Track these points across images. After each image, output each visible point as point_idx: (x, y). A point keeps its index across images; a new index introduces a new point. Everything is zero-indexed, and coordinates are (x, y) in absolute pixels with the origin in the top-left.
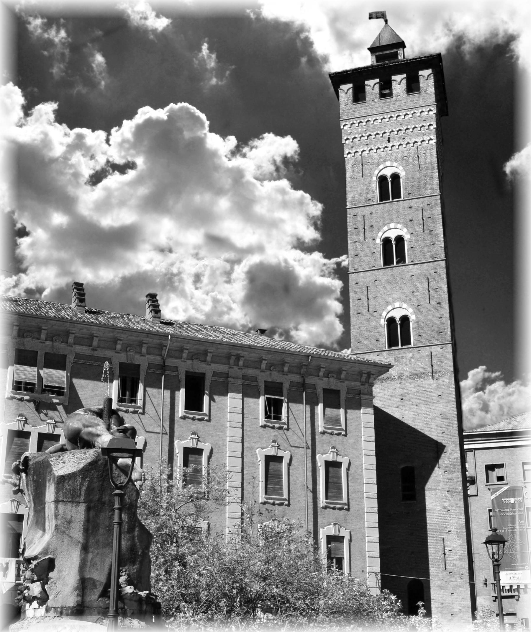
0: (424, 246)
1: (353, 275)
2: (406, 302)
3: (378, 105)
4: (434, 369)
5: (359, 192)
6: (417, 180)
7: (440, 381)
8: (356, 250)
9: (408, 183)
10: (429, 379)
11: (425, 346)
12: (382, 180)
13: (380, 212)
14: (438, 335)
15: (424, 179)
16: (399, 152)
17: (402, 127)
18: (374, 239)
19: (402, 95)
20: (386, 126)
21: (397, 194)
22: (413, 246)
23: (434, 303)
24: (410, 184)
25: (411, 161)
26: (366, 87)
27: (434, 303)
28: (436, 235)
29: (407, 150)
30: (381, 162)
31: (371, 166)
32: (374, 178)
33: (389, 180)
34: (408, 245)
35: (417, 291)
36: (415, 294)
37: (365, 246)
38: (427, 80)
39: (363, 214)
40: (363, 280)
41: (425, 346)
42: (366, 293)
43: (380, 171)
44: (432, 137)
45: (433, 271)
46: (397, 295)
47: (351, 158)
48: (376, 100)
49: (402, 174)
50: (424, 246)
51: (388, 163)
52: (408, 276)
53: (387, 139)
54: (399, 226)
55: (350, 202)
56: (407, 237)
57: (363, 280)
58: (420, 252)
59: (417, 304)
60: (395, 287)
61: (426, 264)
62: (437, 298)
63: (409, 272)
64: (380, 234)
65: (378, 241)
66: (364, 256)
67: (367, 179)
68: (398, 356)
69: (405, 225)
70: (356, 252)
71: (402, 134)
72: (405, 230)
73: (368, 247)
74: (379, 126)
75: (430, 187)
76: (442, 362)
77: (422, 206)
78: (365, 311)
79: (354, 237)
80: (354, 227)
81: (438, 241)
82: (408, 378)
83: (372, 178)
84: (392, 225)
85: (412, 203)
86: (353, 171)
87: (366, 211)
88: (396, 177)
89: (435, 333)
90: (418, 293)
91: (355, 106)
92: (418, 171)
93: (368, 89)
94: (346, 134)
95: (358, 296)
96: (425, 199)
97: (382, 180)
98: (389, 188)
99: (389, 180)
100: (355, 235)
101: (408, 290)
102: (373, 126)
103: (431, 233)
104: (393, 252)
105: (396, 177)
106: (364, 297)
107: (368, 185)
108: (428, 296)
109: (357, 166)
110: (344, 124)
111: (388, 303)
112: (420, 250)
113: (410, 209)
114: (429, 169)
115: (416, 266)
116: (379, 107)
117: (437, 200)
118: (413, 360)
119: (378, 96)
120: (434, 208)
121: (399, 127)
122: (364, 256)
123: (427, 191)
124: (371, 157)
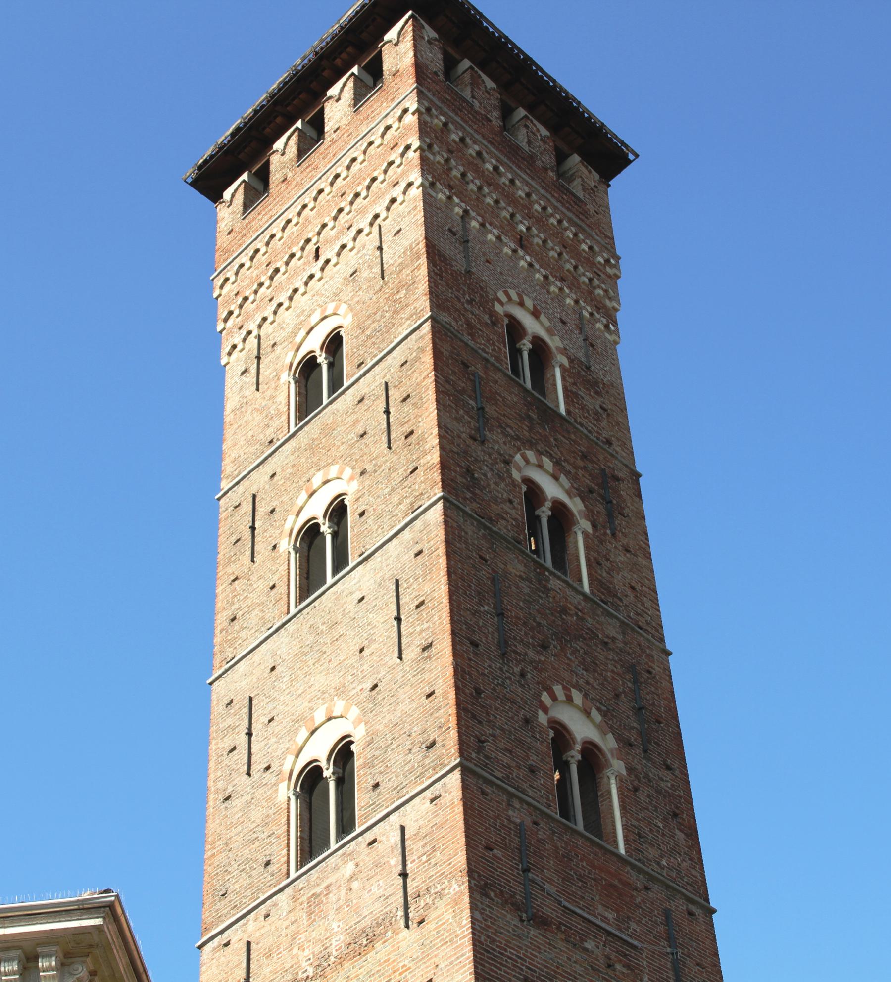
0: (393, 490)
4: (412, 885)
7: (430, 926)
10: (396, 932)
11: (387, 815)
14: (425, 757)
23: (411, 653)
35: (372, 641)
36: (366, 652)
37: (254, 578)
41: (387, 815)
46: (320, 681)
54: (333, 471)
59: (369, 685)
62: (422, 631)
68: (318, 890)
73: (260, 578)
76: (434, 849)
81: (425, 453)
82: (341, 960)
89: (417, 756)
90: (374, 646)
95: (227, 744)
118: (355, 885)
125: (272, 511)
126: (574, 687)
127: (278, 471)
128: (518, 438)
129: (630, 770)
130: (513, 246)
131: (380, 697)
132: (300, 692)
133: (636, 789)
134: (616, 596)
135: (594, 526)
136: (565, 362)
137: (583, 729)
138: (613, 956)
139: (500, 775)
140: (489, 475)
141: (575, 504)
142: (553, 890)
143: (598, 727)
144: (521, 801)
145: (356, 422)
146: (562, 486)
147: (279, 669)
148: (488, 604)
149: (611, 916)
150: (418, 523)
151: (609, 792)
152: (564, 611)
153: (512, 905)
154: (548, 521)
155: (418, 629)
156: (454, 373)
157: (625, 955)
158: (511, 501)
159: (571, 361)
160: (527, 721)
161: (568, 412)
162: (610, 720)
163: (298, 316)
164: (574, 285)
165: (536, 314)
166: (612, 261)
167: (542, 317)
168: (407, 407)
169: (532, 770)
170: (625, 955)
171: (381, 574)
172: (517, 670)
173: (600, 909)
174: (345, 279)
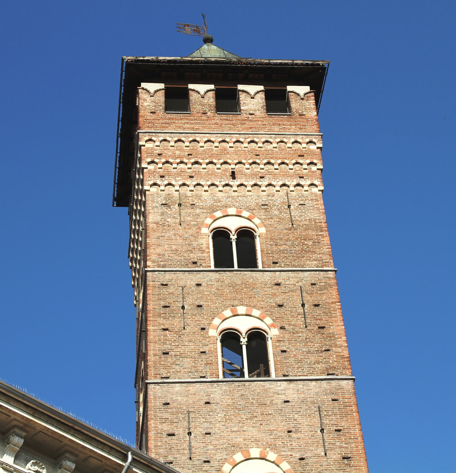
0: (309, 352)
1: (157, 387)
2: (274, 448)
3: (213, 122)
5: (174, 247)
6: (289, 243)
8: (165, 343)
9: (271, 245)
12: (220, 236)
13: (215, 283)
15: (303, 244)
16: (254, 197)
17: (259, 159)
18: (203, 329)
19: (258, 113)
20: (228, 153)
21: (248, 261)
22: (284, 349)
24: (275, 248)
25: (276, 212)
26: (191, 92)
27: (334, 456)
28: (331, 336)
29: (268, 196)
30: (218, 206)
31: (198, 211)
32: (205, 230)
33: (233, 237)
34: (274, 347)
37: (185, 338)
38: (302, 99)
39: (182, 283)
40: (179, 398)
42: (186, 424)
43: (215, 221)
44: (316, 182)
45: (330, 397)
47: (158, 194)
48: (209, 113)
49: (260, 231)
50: (309, 352)
51: (232, 211)
52: (280, 402)
53: (229, 174)
54: (256, 313)
55: (154, 262)
56: (273, 333)
57: (179, 398)
58: (300, 361)
59: (298, 456)
60: (251, 419)
61: (314, 383)
63: (278, 394)
64: (217, 321)
65: (214, 333)
66: (182, 356)
67: (190, 228)
69: (267, 312)
70: (166, 347)
71: (259, 170)
72: (268, 320)
73: (190, 341)
74: (214, 152)
75: (315, 256)
77: (300, 284)
78: (185, 458)
79: (161, 320)
80: (163, 303)
81: (336, 346)
83: (200, 228)
84: (241, 310)
85: (280, 277)
86: (162, 214)
87: (190, 280)
88: (246, 235)
90: (299, 435)
91: (169, 116)
92: (290, 229)
93: (193, 97)
94: (150, 152)
95: (167, 428)
96: (306, 274)
97: (220, 236)
98: (234, 250)
99: (233, 237)
100: (164, 318)
101: (279, 425)
102: (204, 151)
103: (321, 330)
104: (249, 354)
105: (246, 235)
106: (181, 431)
107: (193, 239)
108: (321, 441)
109: (169, 207)
110: (147, 138)
111: (234, 448)
112: (300, 357)
113: (277, 287)
114: (312, 229)
115: (292, 385)
116: (216, 124)
117: (329, 278)
119: (213, 108)
120: (325, 291)
121: (251, 158)
122: (182, 356)
123: (308, 262)
124: (199, 197)
125: (200, 306)
127: (204, 284)
131: (308, 468)
132: (235, 429)
145: (274, 295)
147: (213, 406)
150: (334, 383)
155: (338, 444)
163: (215, 201)
168: (318, 311)
171: (302, 396)
174: (257, 204)
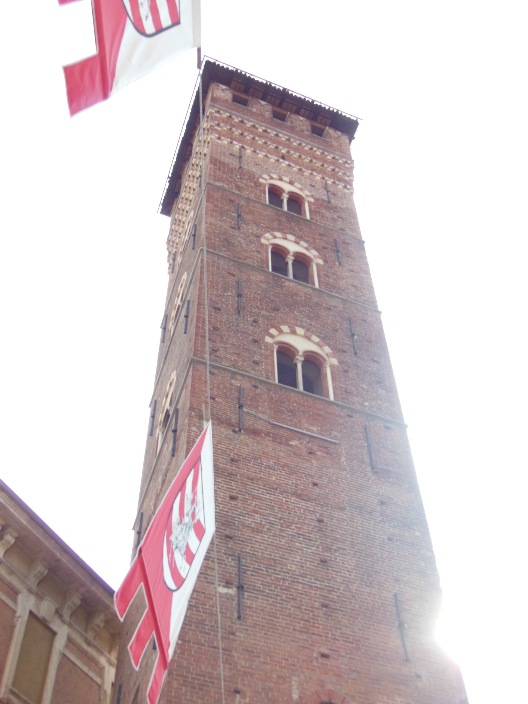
126: (298, 326)
128: (269, 228)
129: (341, 362)
130: (276, 158)
133: (346, 371)
134: (340, 289)
135: (325, 261)
136: (312, 200)
137: (302, 344)
138: (315, 448)
139: (227, 364)
140: (242, 241)
141: (311, 253)
142: (265, 417)
143: (317, 344)
144: (243, 376)
146: (302, 246)
148: (232, 292)
149: (315, 429)
151: (326, 374)
152: (296, 295)
153: (227, 424)
154: (293, 264)
156: (222, 204)
157: (326, 448)
158: (258, 252)
159: (316, 199)
160: (255, 341)
161: (311, 218)
162: (325, 340)
164: (322, 171)
165: (291, 183)
166: (349, 162)
167: (296, 184)
169: (256, 363)
170: (326, 448)
172: (251, 319)
173: (306, 425)
